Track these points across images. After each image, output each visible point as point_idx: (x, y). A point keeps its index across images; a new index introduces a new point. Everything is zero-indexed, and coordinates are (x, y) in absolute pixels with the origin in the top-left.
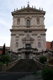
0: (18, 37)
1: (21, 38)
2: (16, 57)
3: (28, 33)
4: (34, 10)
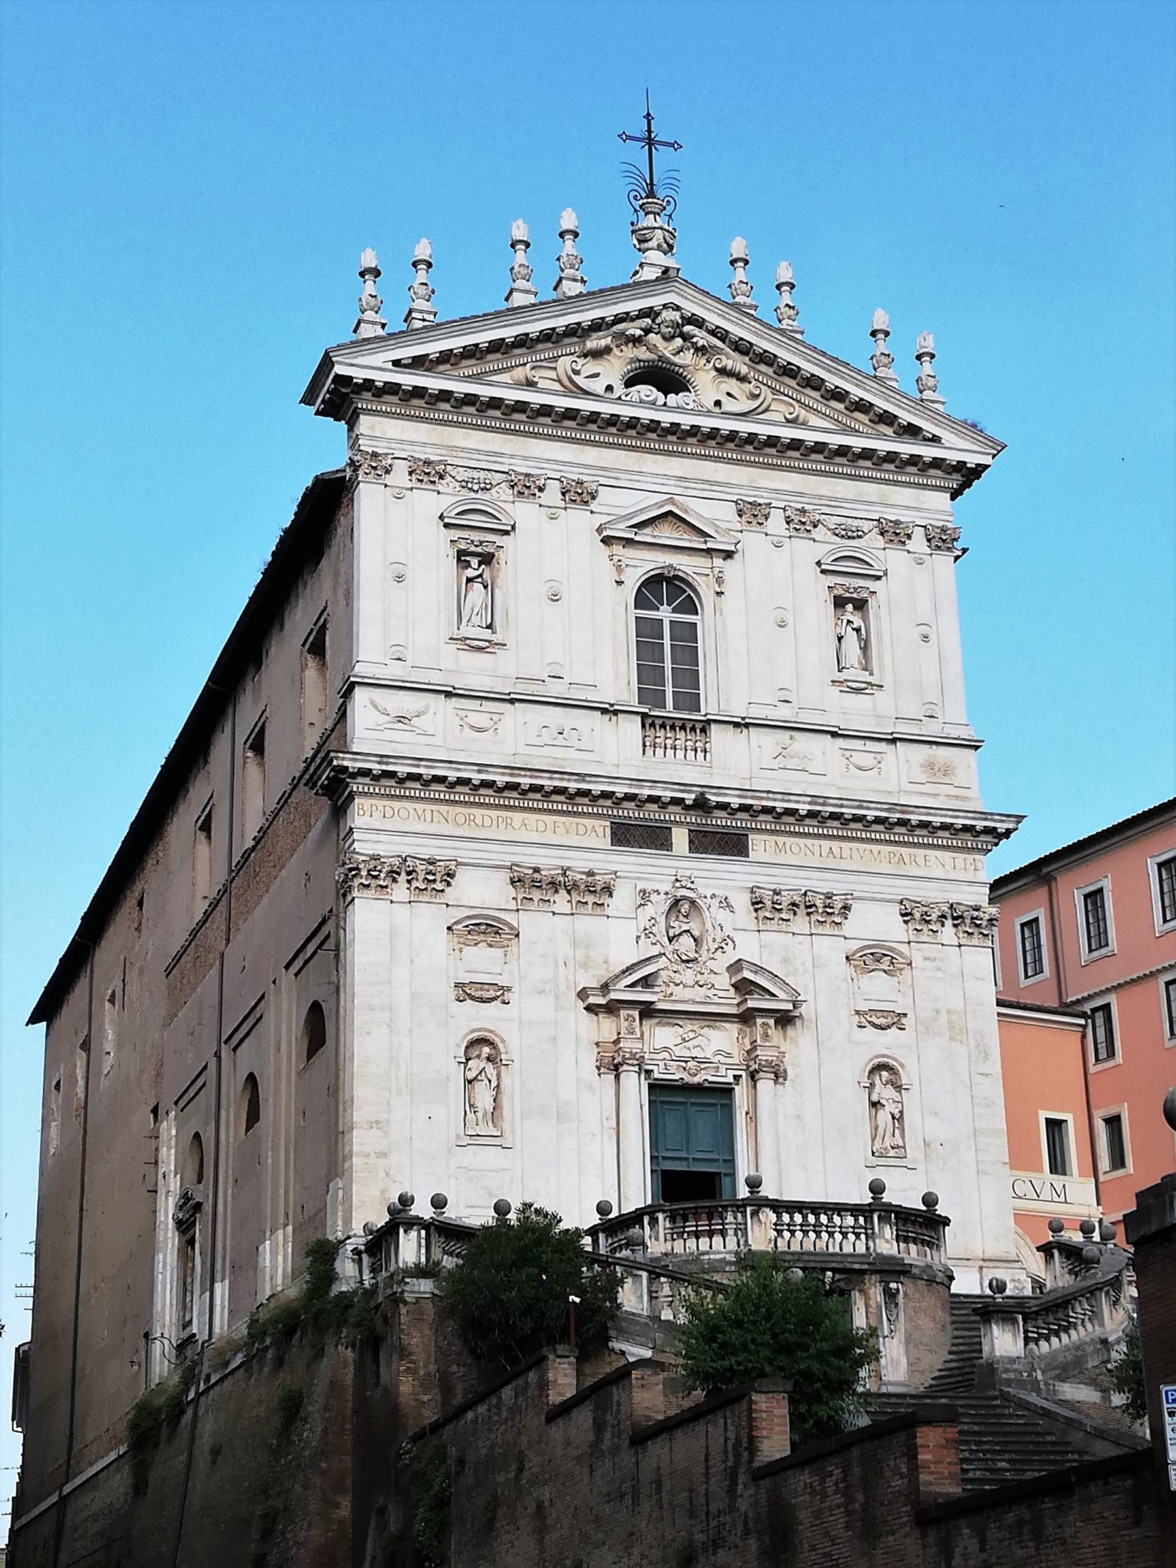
0: (486, 929)
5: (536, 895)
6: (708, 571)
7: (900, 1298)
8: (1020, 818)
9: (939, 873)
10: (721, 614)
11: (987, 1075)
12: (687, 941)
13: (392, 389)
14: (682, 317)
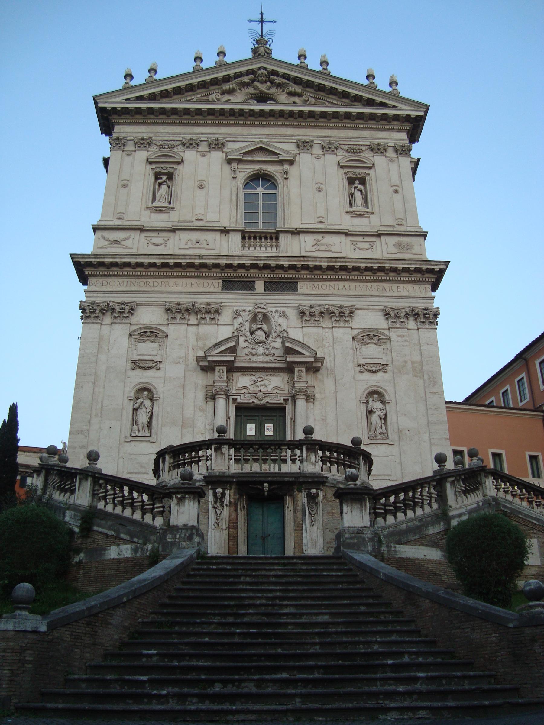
0: (151, 333)
1: (187, 340)
2: (145, 530)
3: (260, 297)
4: (321, 88)
5: (178, 316)
6: (281, 171)
7: (320, 498)
8: (447, 263)
9: (405, 294)
10: (287, 187)
11: (435, 393)
12: (260, 333)
13: (125, 111)
14: (268, 72)
